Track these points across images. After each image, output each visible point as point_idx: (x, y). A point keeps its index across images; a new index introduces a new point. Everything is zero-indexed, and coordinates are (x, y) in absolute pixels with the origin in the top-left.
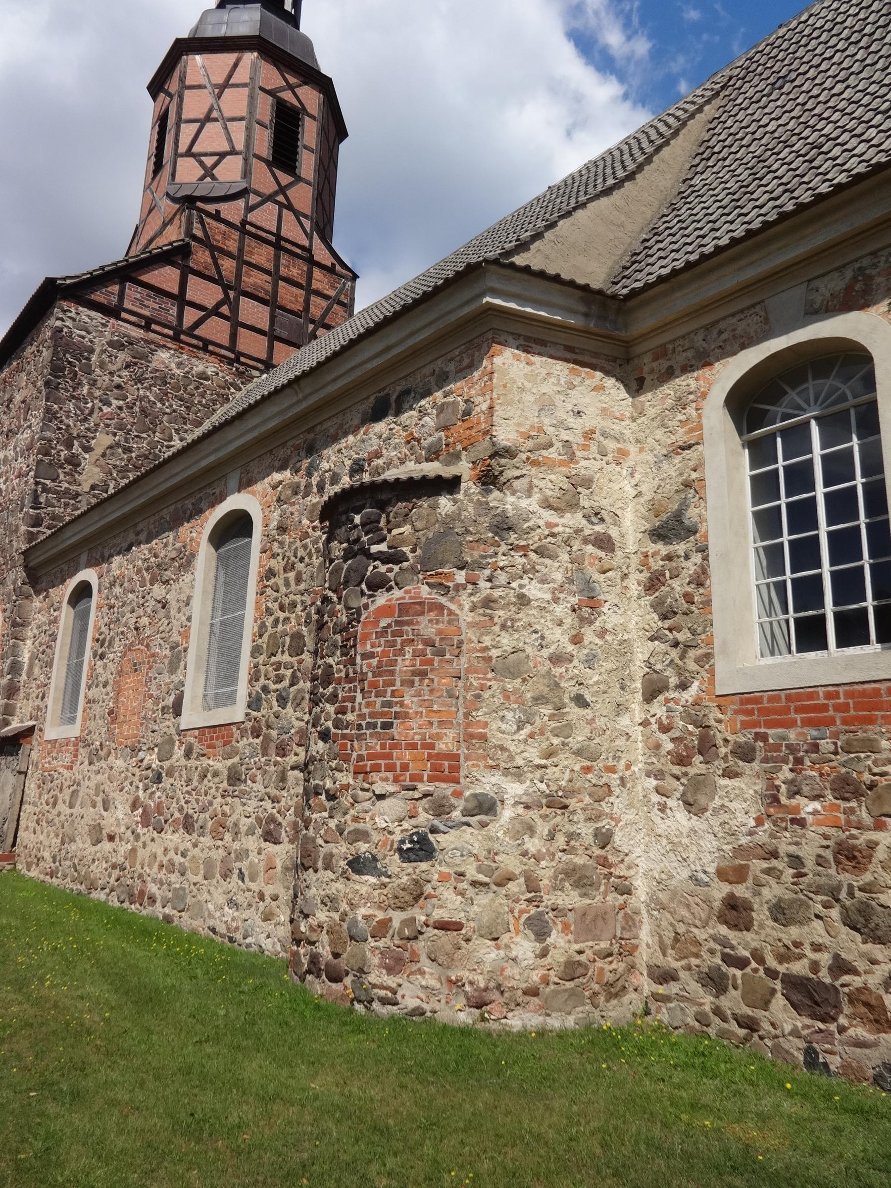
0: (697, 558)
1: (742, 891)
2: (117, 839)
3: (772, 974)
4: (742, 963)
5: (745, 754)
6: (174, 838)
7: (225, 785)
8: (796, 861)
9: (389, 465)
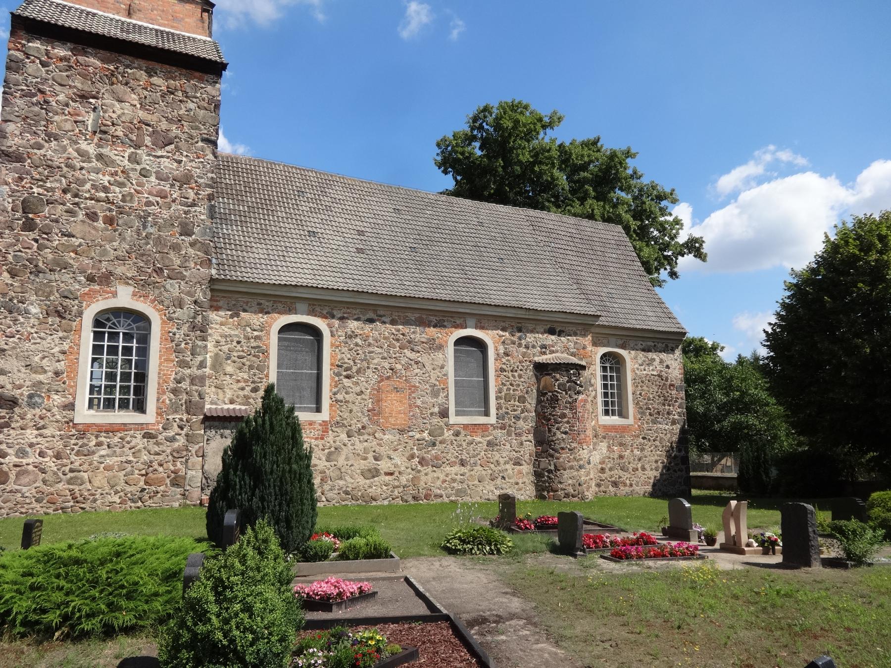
0: (594, 392)
1: (604, 466)
2: (397, 474)
3: (609, 481)
4: (603, 480)
5: (604, 438)
6: (457, 469)
7: (485, 447)
8: (614, 459)
9: (557, 351)
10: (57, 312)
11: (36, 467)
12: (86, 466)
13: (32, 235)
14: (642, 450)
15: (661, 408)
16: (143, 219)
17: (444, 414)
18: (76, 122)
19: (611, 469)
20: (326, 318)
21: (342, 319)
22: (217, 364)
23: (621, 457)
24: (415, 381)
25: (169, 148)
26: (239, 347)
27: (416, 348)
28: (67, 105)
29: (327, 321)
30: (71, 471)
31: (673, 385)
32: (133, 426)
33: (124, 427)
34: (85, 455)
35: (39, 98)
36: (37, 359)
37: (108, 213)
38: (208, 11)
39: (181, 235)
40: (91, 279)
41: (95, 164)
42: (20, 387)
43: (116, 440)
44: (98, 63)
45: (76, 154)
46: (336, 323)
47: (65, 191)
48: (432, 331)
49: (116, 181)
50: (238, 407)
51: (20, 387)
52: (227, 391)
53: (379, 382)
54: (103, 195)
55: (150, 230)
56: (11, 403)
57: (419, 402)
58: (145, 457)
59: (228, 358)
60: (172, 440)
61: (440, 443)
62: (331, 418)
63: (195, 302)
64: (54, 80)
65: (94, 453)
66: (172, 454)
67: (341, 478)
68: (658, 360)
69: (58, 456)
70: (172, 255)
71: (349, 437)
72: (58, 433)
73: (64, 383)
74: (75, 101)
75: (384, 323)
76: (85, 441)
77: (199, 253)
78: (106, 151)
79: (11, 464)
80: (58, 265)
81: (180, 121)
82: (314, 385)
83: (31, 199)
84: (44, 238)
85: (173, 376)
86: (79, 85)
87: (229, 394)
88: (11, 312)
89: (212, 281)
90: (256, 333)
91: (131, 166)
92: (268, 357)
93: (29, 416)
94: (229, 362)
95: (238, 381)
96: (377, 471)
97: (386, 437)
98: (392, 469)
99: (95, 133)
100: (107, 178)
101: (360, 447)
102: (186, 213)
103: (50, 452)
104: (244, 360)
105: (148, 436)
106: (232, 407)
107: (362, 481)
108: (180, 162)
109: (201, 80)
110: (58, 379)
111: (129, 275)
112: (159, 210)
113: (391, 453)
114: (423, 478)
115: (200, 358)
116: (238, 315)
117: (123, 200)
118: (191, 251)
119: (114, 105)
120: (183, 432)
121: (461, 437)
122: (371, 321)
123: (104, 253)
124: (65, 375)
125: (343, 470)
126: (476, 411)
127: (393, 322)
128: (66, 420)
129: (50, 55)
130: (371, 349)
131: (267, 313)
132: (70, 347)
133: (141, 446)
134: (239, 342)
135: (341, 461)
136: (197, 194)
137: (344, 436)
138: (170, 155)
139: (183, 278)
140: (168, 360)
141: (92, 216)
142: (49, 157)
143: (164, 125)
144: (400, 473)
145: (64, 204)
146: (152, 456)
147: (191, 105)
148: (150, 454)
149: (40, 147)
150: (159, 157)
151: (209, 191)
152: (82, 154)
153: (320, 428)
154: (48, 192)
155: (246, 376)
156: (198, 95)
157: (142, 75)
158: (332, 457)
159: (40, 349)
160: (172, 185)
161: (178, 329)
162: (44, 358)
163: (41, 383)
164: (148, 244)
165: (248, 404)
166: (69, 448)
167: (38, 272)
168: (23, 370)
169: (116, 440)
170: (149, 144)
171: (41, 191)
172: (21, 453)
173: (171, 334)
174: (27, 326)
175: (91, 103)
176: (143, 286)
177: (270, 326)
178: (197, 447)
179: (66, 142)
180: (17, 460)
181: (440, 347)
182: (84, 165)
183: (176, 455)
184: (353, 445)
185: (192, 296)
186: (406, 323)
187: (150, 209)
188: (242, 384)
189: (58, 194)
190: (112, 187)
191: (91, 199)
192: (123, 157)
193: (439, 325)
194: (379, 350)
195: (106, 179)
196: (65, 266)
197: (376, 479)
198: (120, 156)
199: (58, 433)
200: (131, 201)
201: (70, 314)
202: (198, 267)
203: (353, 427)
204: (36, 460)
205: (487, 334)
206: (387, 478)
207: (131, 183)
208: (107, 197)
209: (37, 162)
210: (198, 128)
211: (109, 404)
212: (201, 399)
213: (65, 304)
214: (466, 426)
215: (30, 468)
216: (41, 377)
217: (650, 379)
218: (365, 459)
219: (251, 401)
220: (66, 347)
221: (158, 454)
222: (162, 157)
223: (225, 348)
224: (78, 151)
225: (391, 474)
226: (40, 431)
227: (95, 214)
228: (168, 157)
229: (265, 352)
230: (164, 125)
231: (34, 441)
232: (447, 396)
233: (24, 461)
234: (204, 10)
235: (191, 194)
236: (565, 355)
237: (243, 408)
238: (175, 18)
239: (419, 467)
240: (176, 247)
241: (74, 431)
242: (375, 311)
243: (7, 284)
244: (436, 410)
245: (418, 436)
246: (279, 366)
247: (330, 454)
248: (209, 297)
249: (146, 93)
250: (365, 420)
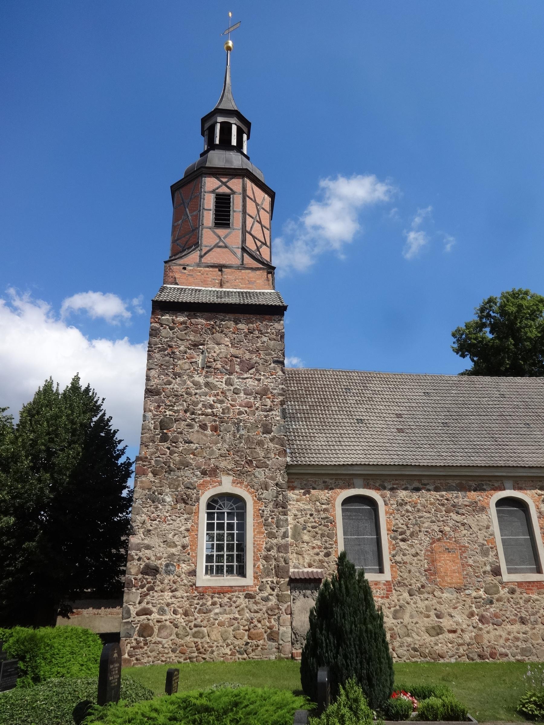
2: (459, 631)
6: (517, 627)
10: (183, 499)
11: (171, 623)
12: (205, 622)
13: (166, 445)
16: (237, 425)
17: (496, 572)
18: (191, 363)
20: (379, 490)
21: (392, 489)
22: (296, 535)
24: (465, 541)
25: (251, 371)
26: (312, 519)
27: (461, 511)
28: (186, 353)
29: (380, 492)
30: (196, 626)
32: (237, 588)
33: (231, 589)
34: (205, 613)
35: (169, 351)
36: (170, 536)
37: (213, 423)
38: (270, 273)
39: (263, 433)
40: (204, 473)
41: (204, 389)
42: (160, 558)
43: (226, 600)
44: (204, 322)
45: (192, 385)
46: (388, 493)
47: (186, 411)
48: (473, 495)
49: (218, 399)
50: (315, 570)
51: (160, 558)
52: (306, 556)
53: (431, 544)
54: (210, 411)
55: (242, 432)
56: (154, 571)
57: (471, 562)
58: (247, 615)
59: (304, 529)
60: (266, 599)
61: (497, 600)
62: (393, 578)
63: (277, 484)
64: (177, 338)
65: (210, 611)
66: (267, 612)
67: (408, 635)
69: (186, 614)
70: (258, 449)
71: (411, 595)
72: (186, 594)
73: (189, 554)
74: (190, 349)
75: (429, 490)
76: (204, 601)
77: (277, 446)
78: (210, 380)
79: (155, 620)
80: (183, 465)
81: (258, 351)
82: (375, 549)
83: (166, 419)
84: (173, 446)
85: (264, 546)
86: (192, 338)
87: (307, 559)
88: (154, 502)
89: (288, 466)
90: (324, 506)
91: (228, 388)
92: (335, 526)
93: (166, 581)
94: (305, 531)
95: (314, 548)
96: (440, 628)
97: (445, 595)
98: (454, 627)
99: (203, 368)
100: (212, 398)
101: (422, 605)
102: (266, 417)
103: (180, 610)
104: (317, 530)
105: (249, 596)
106: (310, 570)
107: (427, 639)
108: (259, 380)
109: (270, 320)
110: (185, 551)
111: (229, 468)
112: (247, 417)
113: (451, 610)
114: (486, 636)
115: (283, 530)
116: (309, 493)
117: (223, 413)
118: (271, 445)
119: (214, 348)
120: (274, 593)
121: (516, 595)
122: (417, 489)
124: (189, 548)
125: (409, 627)
126: (527, 568)
127: (437, 489)
128: (191, 584)
129: (175, 322)
130: (420, 514)
131: (331, 489)
132: (192, 526)
133: (244, 605)
134: (311, 515)
135: (407, 619)
136: (273, 401)
137: (406, 595)
138: (252, 376)
139: (267, 466)
140: (260, 533)
141: (203, 427)
142: (175, 389)
143: (247, 356)
144: (462, 630)
145: (185, 420)
146: (252, 614)
147: (265, 339)
148: (251, 612)
149: (169, 383)
150: (245, 379)
151: (281, 398)
152: (197, 384)
153: (384, 587)
154: (175, 413)
155: (319, 543)
156: (269, 331)
157: (232, 324)
158: (399, 615)
159: (173, 528)
160: (255, 398)
161: (265, 507)
162: (175, 535)
163: (174, 555)
164: (241, 442)
165: (322, 567)
166: (193, 607)
167: (170, 470)
168: (162, 545)
169: (226, 600)
170: (238, 370)
171: (171, 413)
172: (162, 611)
173: (261, 512)
174: (164, 511)
175: (200, 349)
177: (335, 500)
178: (286, 606)
179: (185, 377)
180: (158, 617)
181: (483, 509)
182: (197, 391)
183: (271, 612)
184: (415, 603)
185: (274, 480)
186: (449, 489)
187: (241, 417)
188: (317, 550)
189: (181, 414)
190: (216, 405)
191: (202, 414)
192: (222, 382)
193: (478, 488)
194: (428, 515)
197: (440, 636)
198: (219, 381)
199: (186, 594)
200: (228, 413)
201: (191, 501)
202: (277, 457)
203: (413, 586)
204: (171, 617)
205: (526, 494)
206: (451, 635)
207: (228, 400)
208: (212, 412)
209: (169, 394)
210: (270, 354)
211: (219, 570)
212: (286, 564)
213: (187, 493)
214: (520, 584)
215: (168, 623)
216: (173, 550)
218: (428, 616)
219: (325, 564)
220: (189, 526)
221: (257, 612)
222: (247, 378)
223: (301, 520)
224: (193, 382)
225: (454, 632)
226: (174, 593)
227: (205, 425)
228: (251, 378)
229: (333, 522)
230: (247, 356)
231: (170, 601)
232: (497, 555)
233: (164, 618)
234: (269, 273)
235: (269, 402)
237: (319, 570)
238: (250, 282)
239: (480, 625)
240: (260, 443)
241: (196, 593)
242: (420, 481)
243: (151, 481)
244: (488, 568)
245: (474, 594)
246: (345, 533)
247: (396, 612)
248: (286, 480)
249: (234, 335)
250: (423, 579)
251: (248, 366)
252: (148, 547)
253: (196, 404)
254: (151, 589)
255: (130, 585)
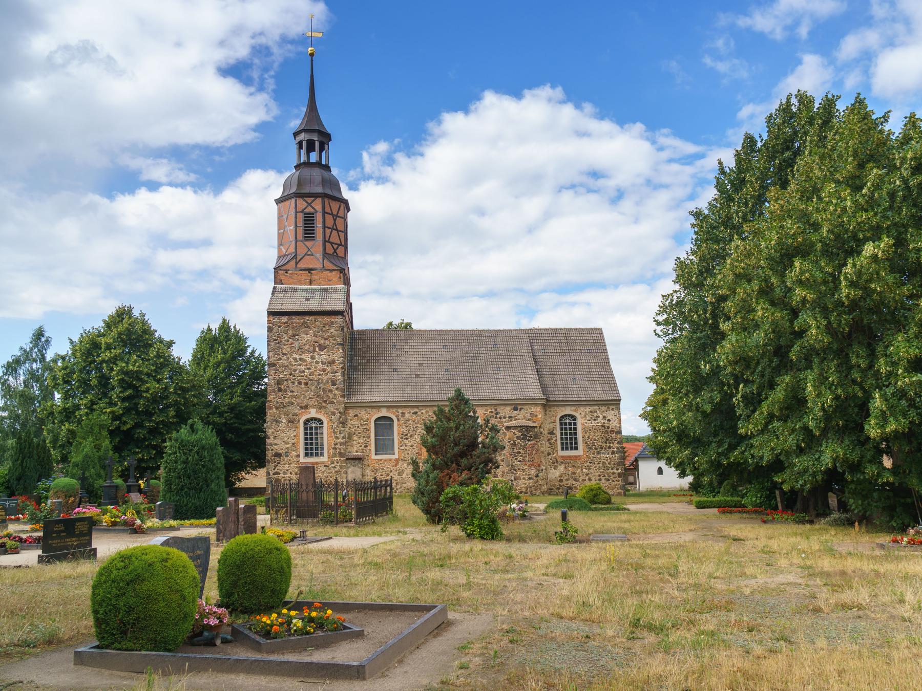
5: (562, 463)
14: (590, 469)
15: (604, 445)
19: (567, 480)
23: (574, 473)
31: (613, 431)
40: (301, 407)
60: (335, 467)
68: (601, 417)
70: (330, 395)
78: (302, 356)
87: (355, 449)
123: (305, 397)
135: (404, 476)
143: (322, 342)
149: (280, 359)
151: (341, 366)
152: (295, 359)
176: (320, 408)
187: (320, 377)
195: (303, 368)
196: (293, 404)
198: (307, 357)
216: (288, 446)
217: (596, 429)
236: (524, 421)
240: (331, 391)
251: (322, 348)
252: (276, 444)
253: (295, 371)
254: (279, 463)
255: (269, 462)
